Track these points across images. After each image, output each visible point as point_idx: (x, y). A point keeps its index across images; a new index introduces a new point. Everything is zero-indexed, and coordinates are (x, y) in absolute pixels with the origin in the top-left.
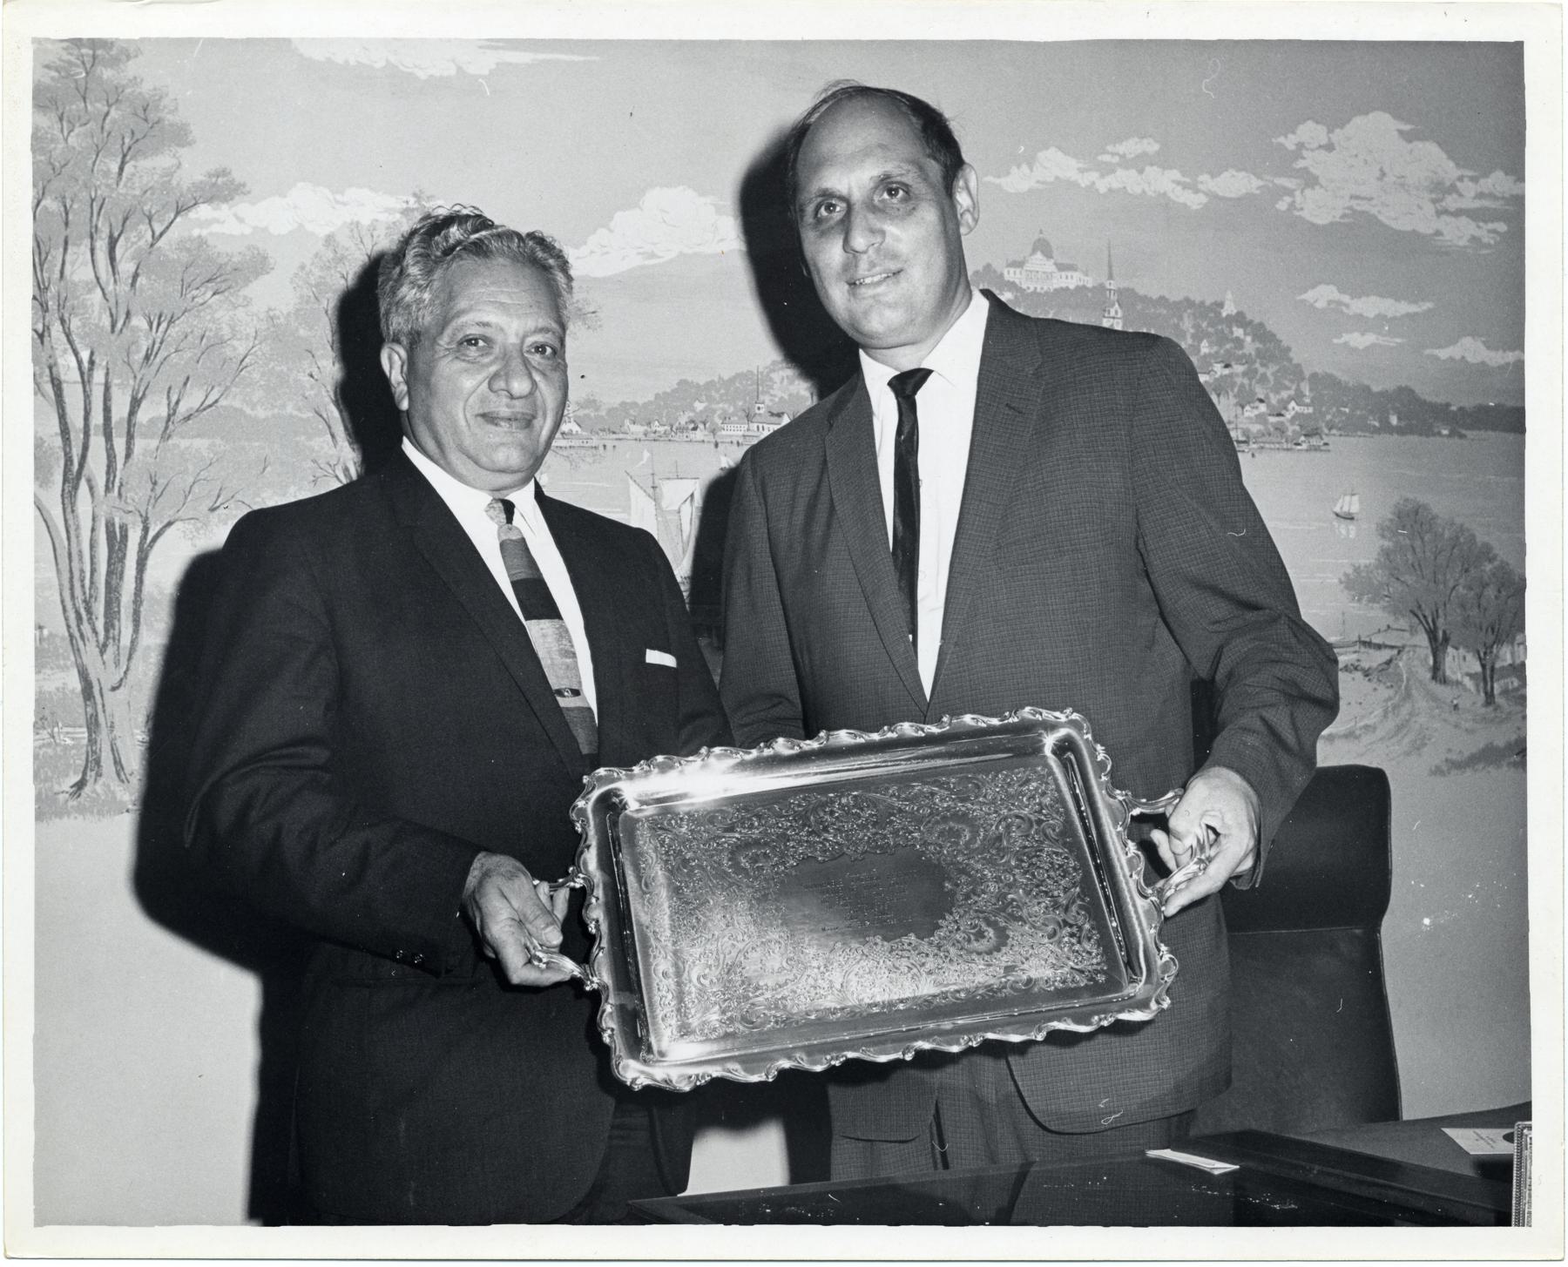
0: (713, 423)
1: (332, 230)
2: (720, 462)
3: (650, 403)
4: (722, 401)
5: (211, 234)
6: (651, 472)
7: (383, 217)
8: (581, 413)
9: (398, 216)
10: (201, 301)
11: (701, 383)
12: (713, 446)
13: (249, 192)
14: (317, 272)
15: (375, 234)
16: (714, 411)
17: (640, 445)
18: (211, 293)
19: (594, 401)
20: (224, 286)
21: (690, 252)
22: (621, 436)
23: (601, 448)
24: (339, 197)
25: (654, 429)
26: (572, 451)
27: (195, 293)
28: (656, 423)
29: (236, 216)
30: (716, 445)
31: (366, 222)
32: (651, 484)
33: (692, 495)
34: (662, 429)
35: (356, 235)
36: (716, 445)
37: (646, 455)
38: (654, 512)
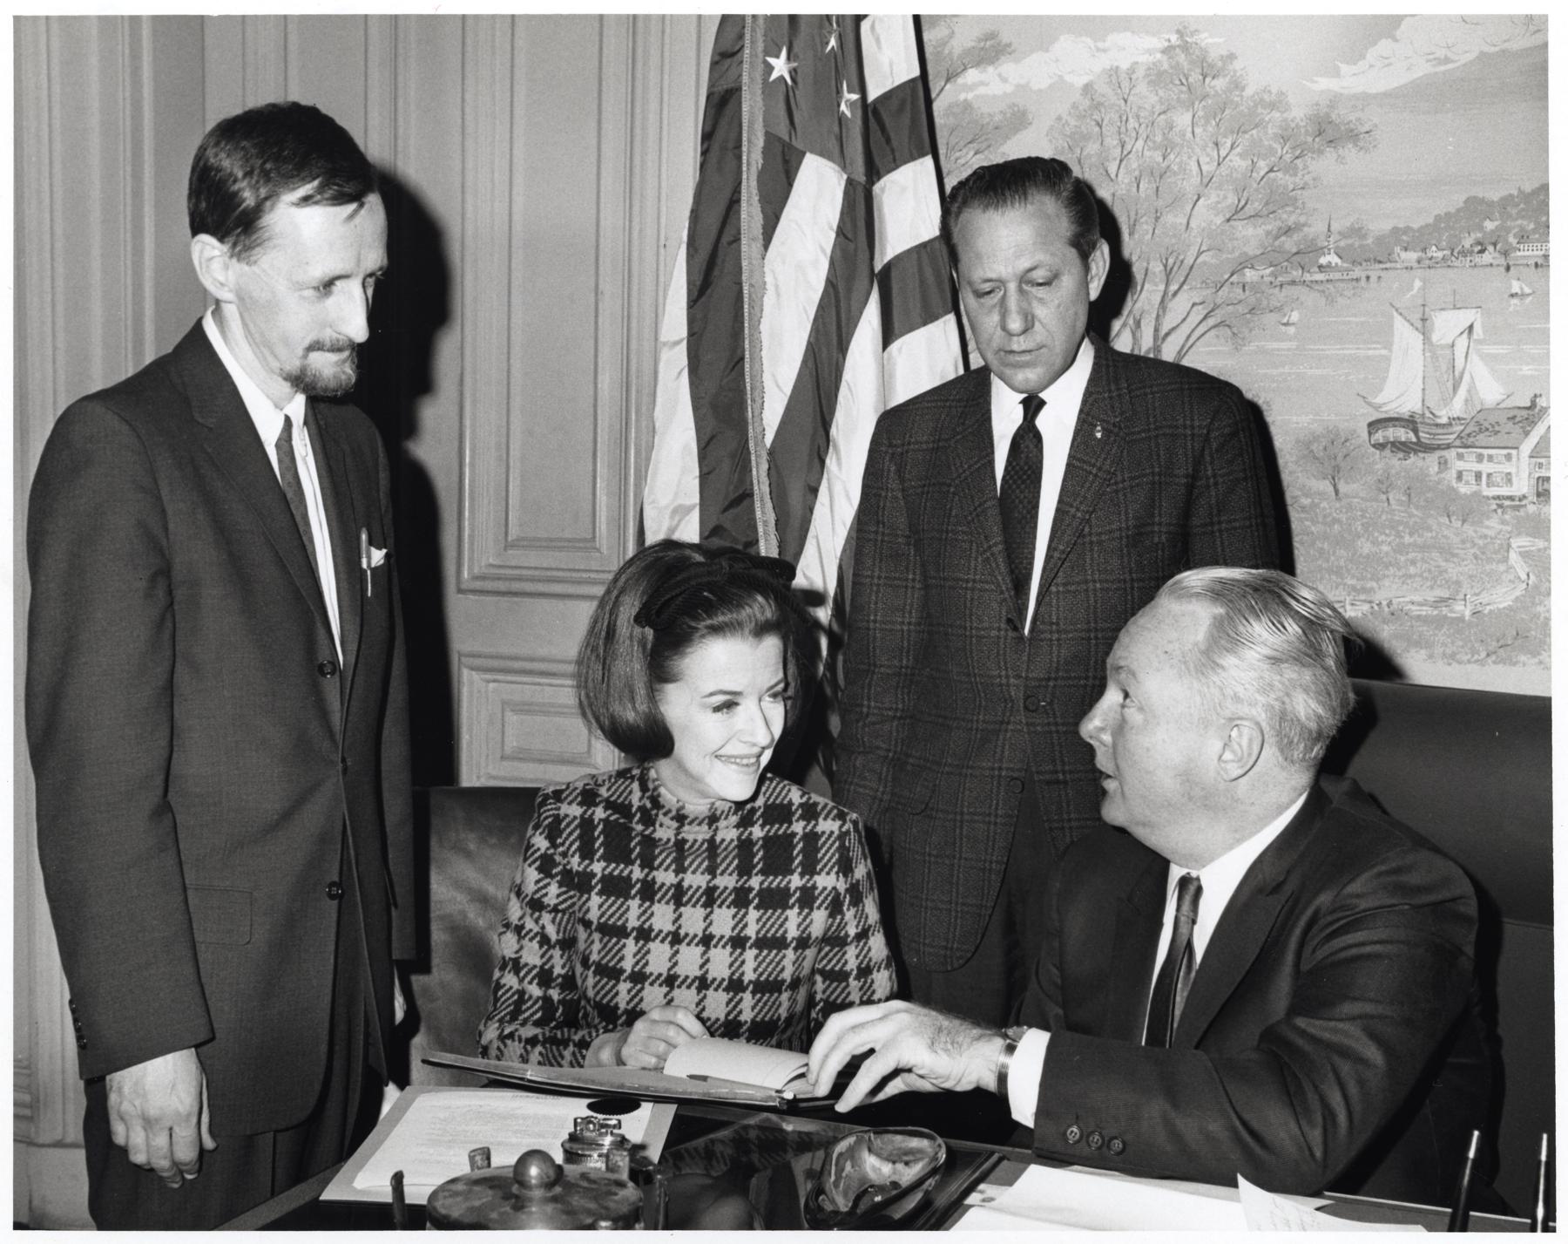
0: (1506, 242)
1: (1091, 78)
2: (1511, 287)
3: (1427, 226)
4: (1520, 216)
5: (977, 97)
6: (1420, 302)
7: (1144, 59)
8: (1342, 244)
9: (1159, 56)
10: (962, 161)
11: (1495, 196)
12: (1502, 269)
13: (1014, 51)
14: (1073, 122)
15: (1134, 77)
16: (1508, 230)
17: (1414, 272)
18: (972, 153)
19: (1360, 229)
20: (984, 145)
21: (1497, 49)
22: (1388, 265)
23: (1364, 279)
24: (1100, 45)
25: (1429, 255)
26: (1330, 286)
27: (958, 154)
28: (1434, 248)
29: (1000, 75)
30: (1508, 268)
31: (1124, 66)
32: (1419, 316)
33: (1471, 327)
34: (1440, 254)
35: (1114, 79)
36: (1508, 268)
37: (1418, 284)
38: (1421, 346)
